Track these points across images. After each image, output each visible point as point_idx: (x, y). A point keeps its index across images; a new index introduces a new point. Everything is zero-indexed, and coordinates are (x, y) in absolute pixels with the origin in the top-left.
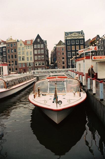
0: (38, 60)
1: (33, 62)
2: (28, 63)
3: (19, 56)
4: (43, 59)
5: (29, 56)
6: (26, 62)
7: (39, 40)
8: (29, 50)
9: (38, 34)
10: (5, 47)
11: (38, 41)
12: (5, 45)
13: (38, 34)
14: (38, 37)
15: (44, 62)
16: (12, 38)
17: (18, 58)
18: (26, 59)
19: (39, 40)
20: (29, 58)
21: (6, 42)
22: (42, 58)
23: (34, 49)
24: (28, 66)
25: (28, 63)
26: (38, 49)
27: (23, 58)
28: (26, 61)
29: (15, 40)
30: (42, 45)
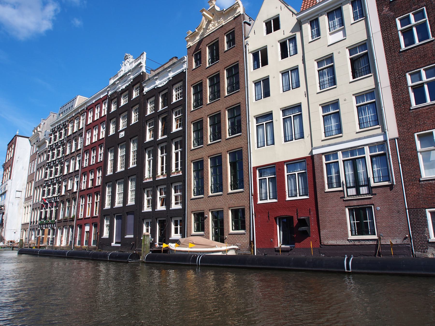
25: (335, 153)
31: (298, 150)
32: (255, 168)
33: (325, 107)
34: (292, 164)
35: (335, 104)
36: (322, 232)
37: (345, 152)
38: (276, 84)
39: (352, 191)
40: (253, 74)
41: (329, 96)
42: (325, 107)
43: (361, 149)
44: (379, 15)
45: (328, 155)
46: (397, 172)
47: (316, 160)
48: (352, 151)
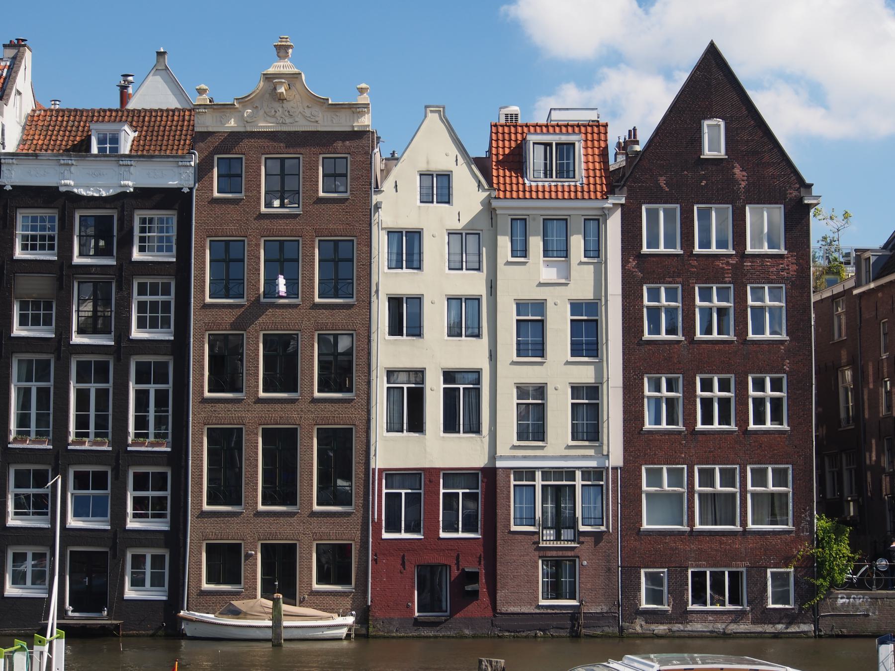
0: (683, 448)
2: (539, 482)
3: (389, 352)
4: (769, 425)
5: (560, 371)
7: (713, 140)
9: (712, 46)
10: (174, 200)
11: (707, 153)
12: (173, 176)
13: (712, 46)
14: (712, 84)
15: (780, 478)
19: (713, 140)
21: (206, 123)
22: (760, 419)
23: (640, 270)
25: (530, 473)
26: (708, 270)
27: (450, 397)
29: (337, 107)
30: (763, 224)
31: (465, 452)
32: (381, 471)
33: (522, 390)
34: (453, 476)
35: (540, 391)
36: (500, 595)
37: (547, 473)
38: (435, 318)
39: (549, 534)
40: (388, 281)
41: (531, 375)
42: (522, 390)
43: (570, 474)
44: (623, 266)
45: (520, 473)
46: (615, 516)
47: (500, 476)
48: (559, 473)
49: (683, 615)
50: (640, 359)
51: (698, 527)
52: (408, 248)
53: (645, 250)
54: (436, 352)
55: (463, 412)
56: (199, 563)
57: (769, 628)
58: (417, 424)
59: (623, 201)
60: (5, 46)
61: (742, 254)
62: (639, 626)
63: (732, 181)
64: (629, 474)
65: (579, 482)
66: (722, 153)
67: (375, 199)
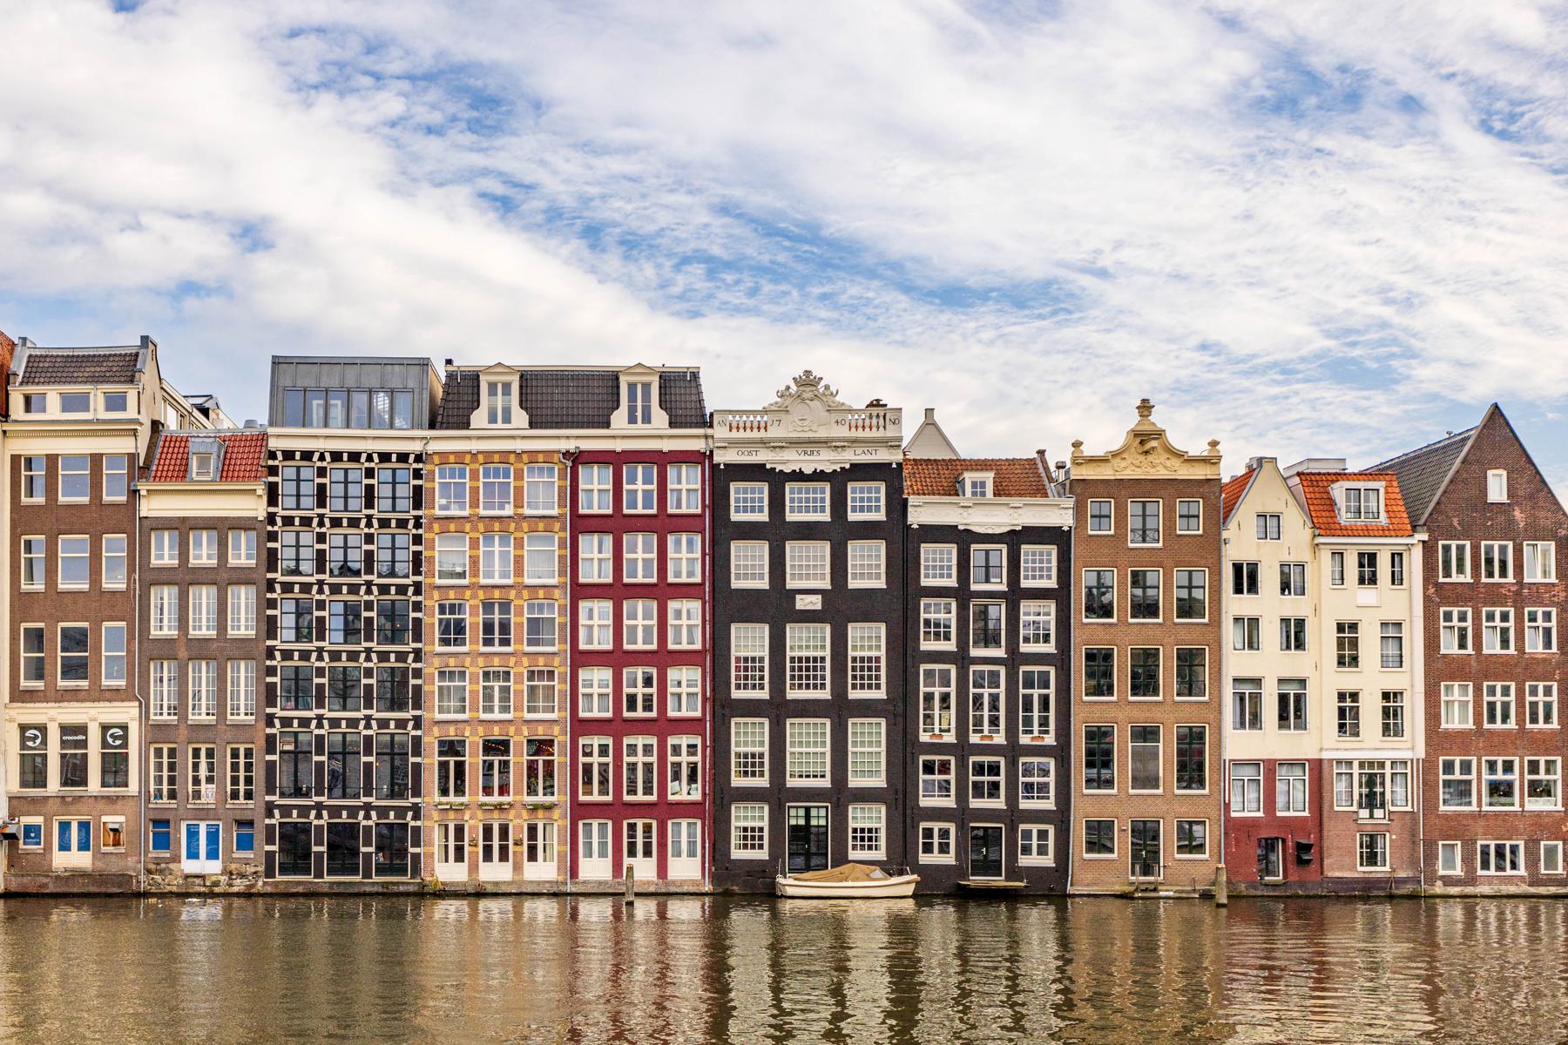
1: (1421, 752)
2: (1356, 770)
3: (1236, 662)
5: (1370, 680)
6: (1325, 755)
7: (1497, 487)
8: (1367, 595)
16: (1158, 418)
17: (1228, 691)
18: (1321, 710)
20: (1370, 712)
23: (1438, 596)
24: (1343, 795)
25: (1349, 763)
27: (1283, 699)
28: (1319, 737)
36: (1326, 862)
39: (1364, 813)
47: (1325, 766)
48: (1371, 764)
49: (1471, 879)
50: (1439, 670)
51: (1485, 808)
52: (1246, 578)
53: (1441, 580)
54: (1270, 663)
55: (1292, 710)
56: (1079, 834)
57: (1542, 890)
58: (1256, 721)
59: (1425, 537)
60: (929, 412)
61: (1520, 583)
62: (1439, 888)
63: (1511, 521)
64: (1428, 765)
65: (1388, 771)
66: (1504, 499)
67: (1225, 535)
